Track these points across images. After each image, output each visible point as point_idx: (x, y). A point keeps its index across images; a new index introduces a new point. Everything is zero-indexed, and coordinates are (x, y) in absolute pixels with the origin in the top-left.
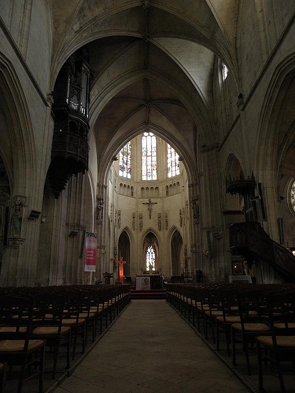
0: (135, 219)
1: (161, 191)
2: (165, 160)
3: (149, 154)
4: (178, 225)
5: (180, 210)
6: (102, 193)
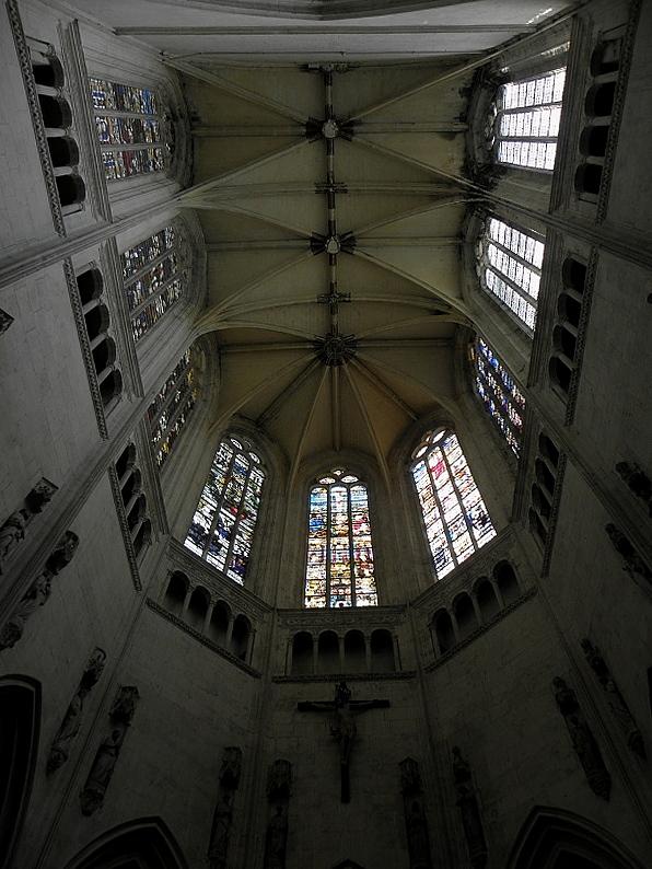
2: (411, 534)
3: (340, 528)
4: (570, 792)
5: (559, 682)
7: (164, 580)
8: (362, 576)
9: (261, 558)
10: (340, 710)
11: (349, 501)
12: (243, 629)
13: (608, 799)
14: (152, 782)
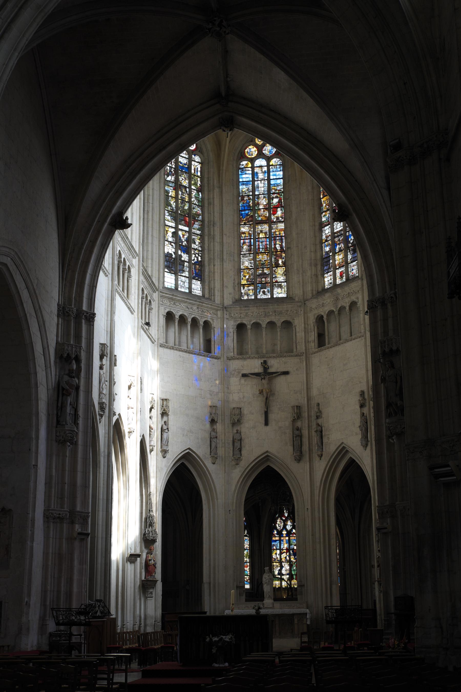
0: (219, 427)
1: (300, 334)
6: (78, 337)
7: (162, 320)
8: (277, 266)
9: (210, 260)
10: (263, 380)
11: (269, 180)
12: (206, 323)
13: (365, 450)
14: (183, 435)
